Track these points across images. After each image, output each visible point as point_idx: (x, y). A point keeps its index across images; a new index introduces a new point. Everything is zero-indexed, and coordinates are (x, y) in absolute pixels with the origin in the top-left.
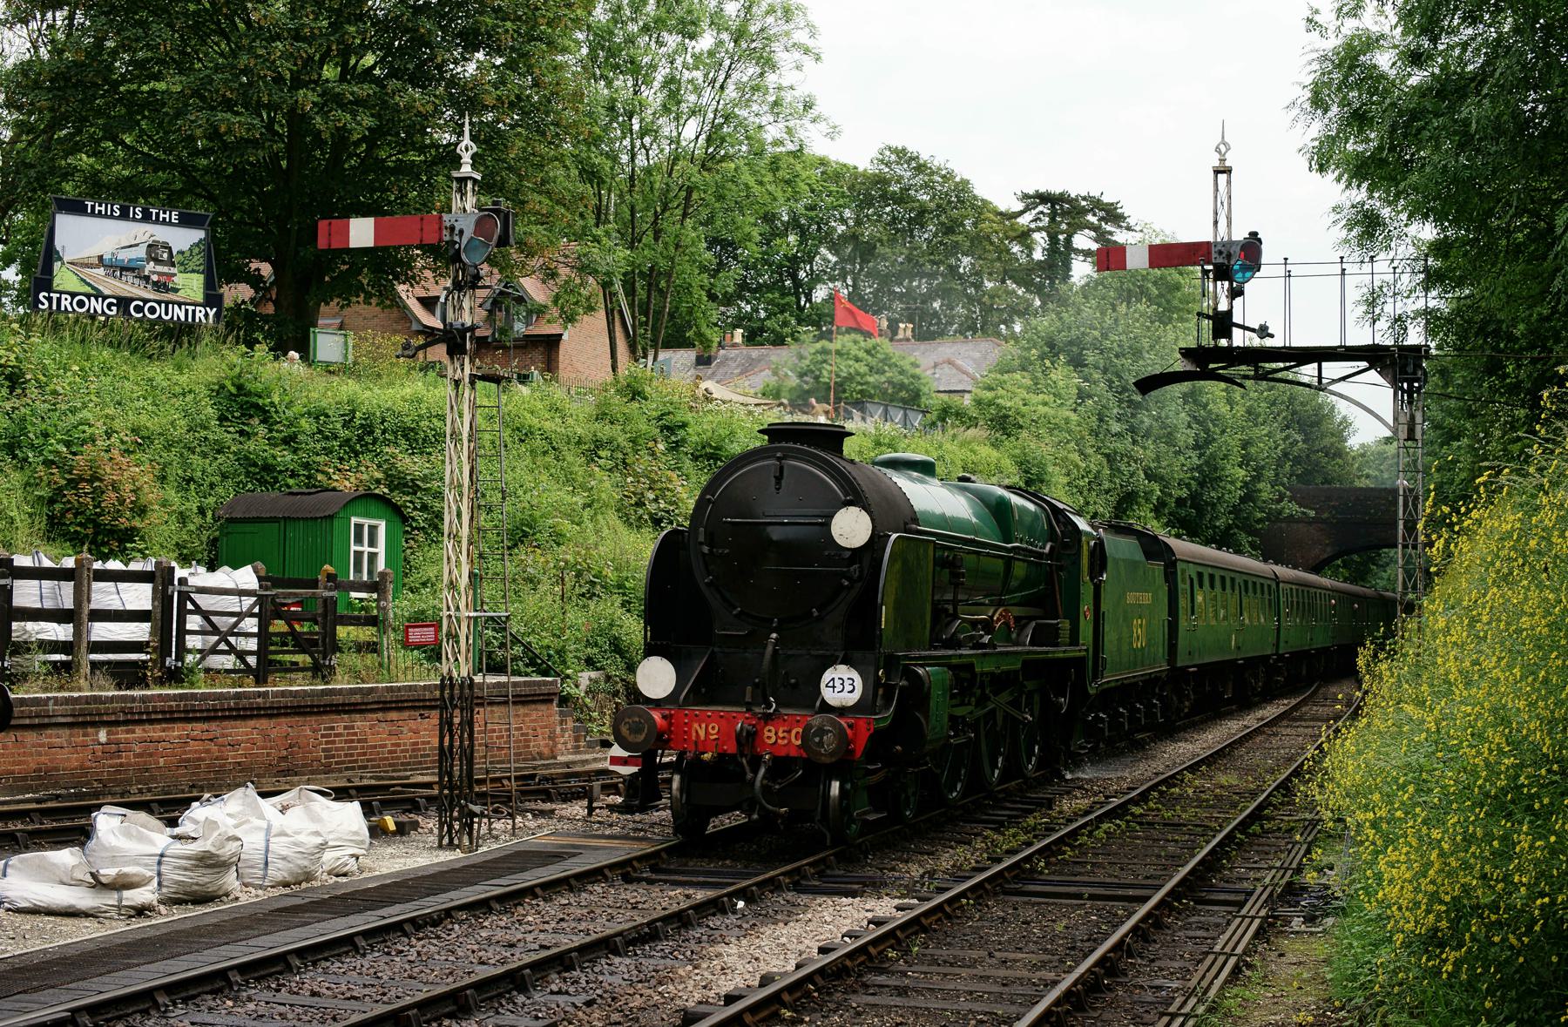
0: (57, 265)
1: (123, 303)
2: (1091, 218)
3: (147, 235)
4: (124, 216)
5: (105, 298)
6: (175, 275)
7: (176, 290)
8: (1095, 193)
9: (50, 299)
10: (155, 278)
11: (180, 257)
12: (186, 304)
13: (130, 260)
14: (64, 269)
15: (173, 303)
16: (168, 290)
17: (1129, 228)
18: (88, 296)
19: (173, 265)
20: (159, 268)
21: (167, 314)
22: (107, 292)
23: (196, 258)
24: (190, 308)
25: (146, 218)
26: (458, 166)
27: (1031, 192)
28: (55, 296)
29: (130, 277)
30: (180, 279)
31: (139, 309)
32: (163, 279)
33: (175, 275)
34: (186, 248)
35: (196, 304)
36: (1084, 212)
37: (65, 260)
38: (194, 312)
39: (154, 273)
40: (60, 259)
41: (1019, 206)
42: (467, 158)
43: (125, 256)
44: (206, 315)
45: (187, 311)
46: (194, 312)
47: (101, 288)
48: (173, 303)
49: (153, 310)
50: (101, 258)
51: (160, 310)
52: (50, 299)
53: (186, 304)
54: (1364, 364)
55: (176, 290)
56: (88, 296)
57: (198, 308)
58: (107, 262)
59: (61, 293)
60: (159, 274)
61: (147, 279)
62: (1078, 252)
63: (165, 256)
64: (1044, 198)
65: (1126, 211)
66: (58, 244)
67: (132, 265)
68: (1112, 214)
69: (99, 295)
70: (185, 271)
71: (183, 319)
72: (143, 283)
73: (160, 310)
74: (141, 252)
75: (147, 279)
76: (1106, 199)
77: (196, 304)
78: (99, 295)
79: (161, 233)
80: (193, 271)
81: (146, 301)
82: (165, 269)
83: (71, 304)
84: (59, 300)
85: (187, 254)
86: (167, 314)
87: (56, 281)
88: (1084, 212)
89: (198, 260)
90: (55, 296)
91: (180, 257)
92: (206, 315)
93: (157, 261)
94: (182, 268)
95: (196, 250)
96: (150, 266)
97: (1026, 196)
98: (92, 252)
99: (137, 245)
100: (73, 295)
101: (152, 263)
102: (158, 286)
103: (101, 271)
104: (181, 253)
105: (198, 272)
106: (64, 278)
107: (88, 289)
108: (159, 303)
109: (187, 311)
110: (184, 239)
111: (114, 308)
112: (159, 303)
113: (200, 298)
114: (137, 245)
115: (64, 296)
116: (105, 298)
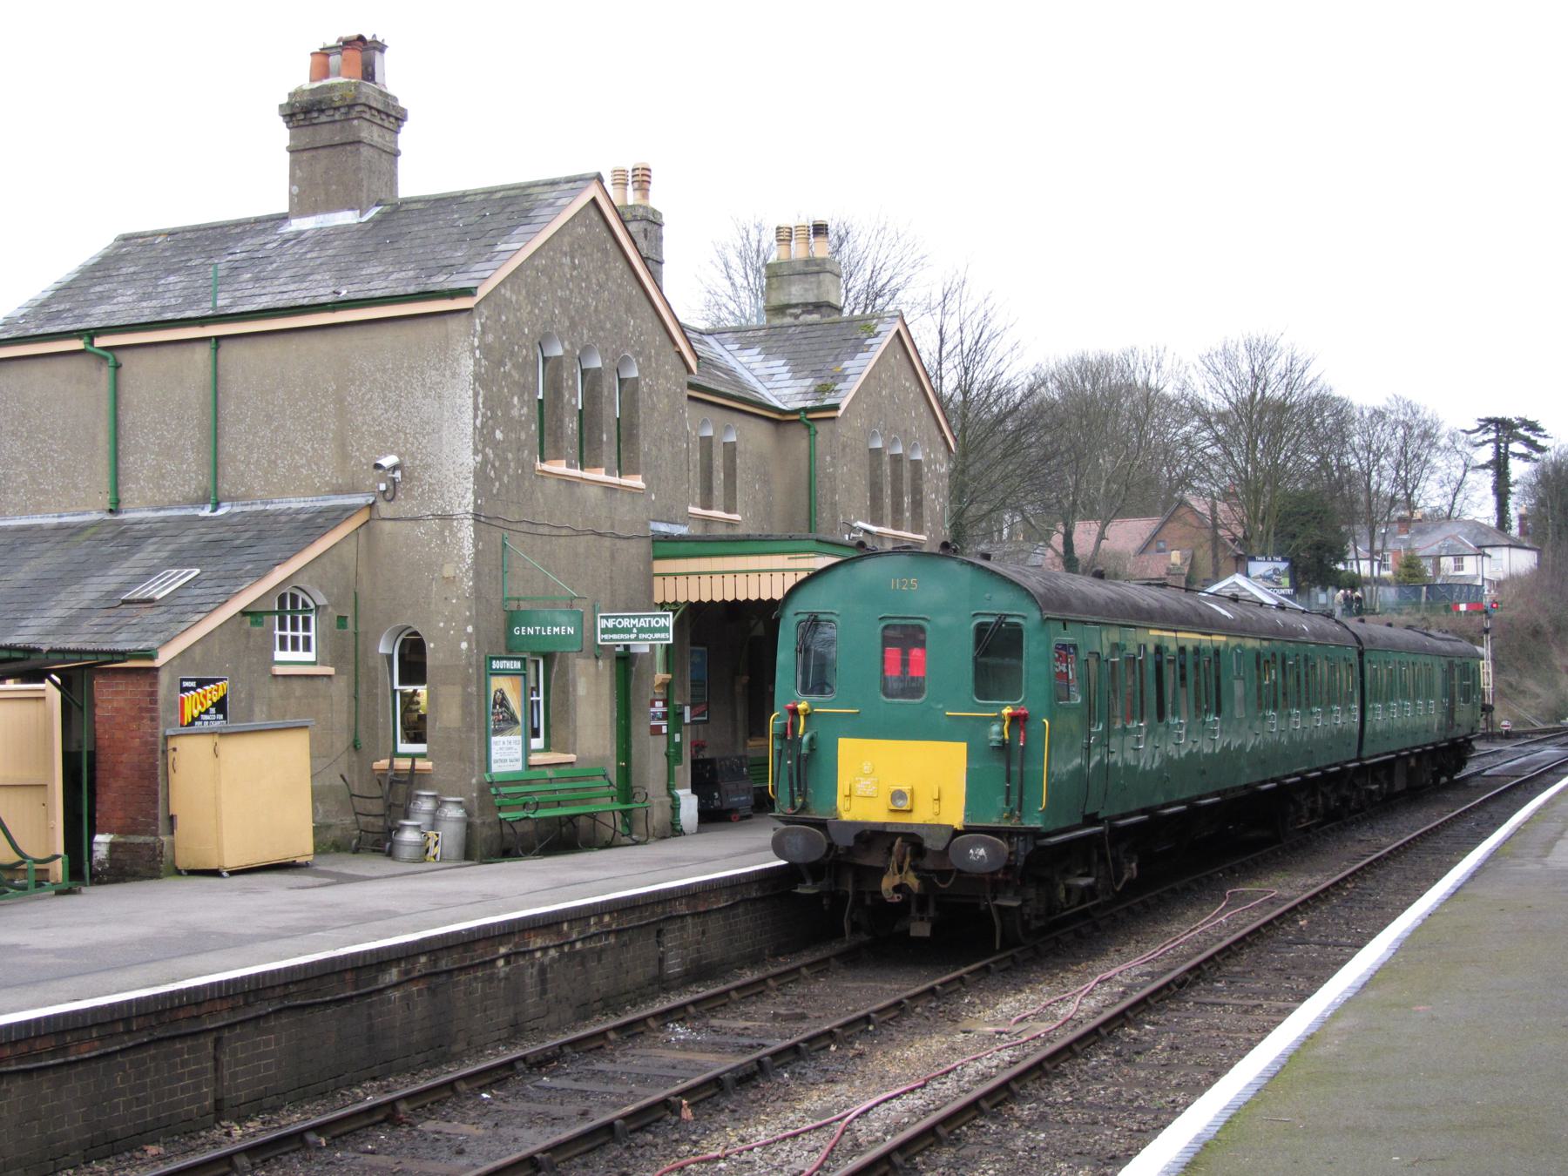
2: (1521, 431)
4: (1266, 560)
8: (1522, 416)
17: (1545, 436)
25: (1272, 560)
27: (1483, 417)
36: (1516, 427)
41: (1477, 427)
43: (1267, 574)
62: (1515, 455)
64: (1490, 421)
65: (1541, 425)
68: (1533, 427)
74: (1271, 572)
76: (1529, 419)
79: (1277, 565)
88: (1516, 427)
89: (1287, 573)
97: (1480, 420)
98: (1258, 574)
102: (1277, 583)
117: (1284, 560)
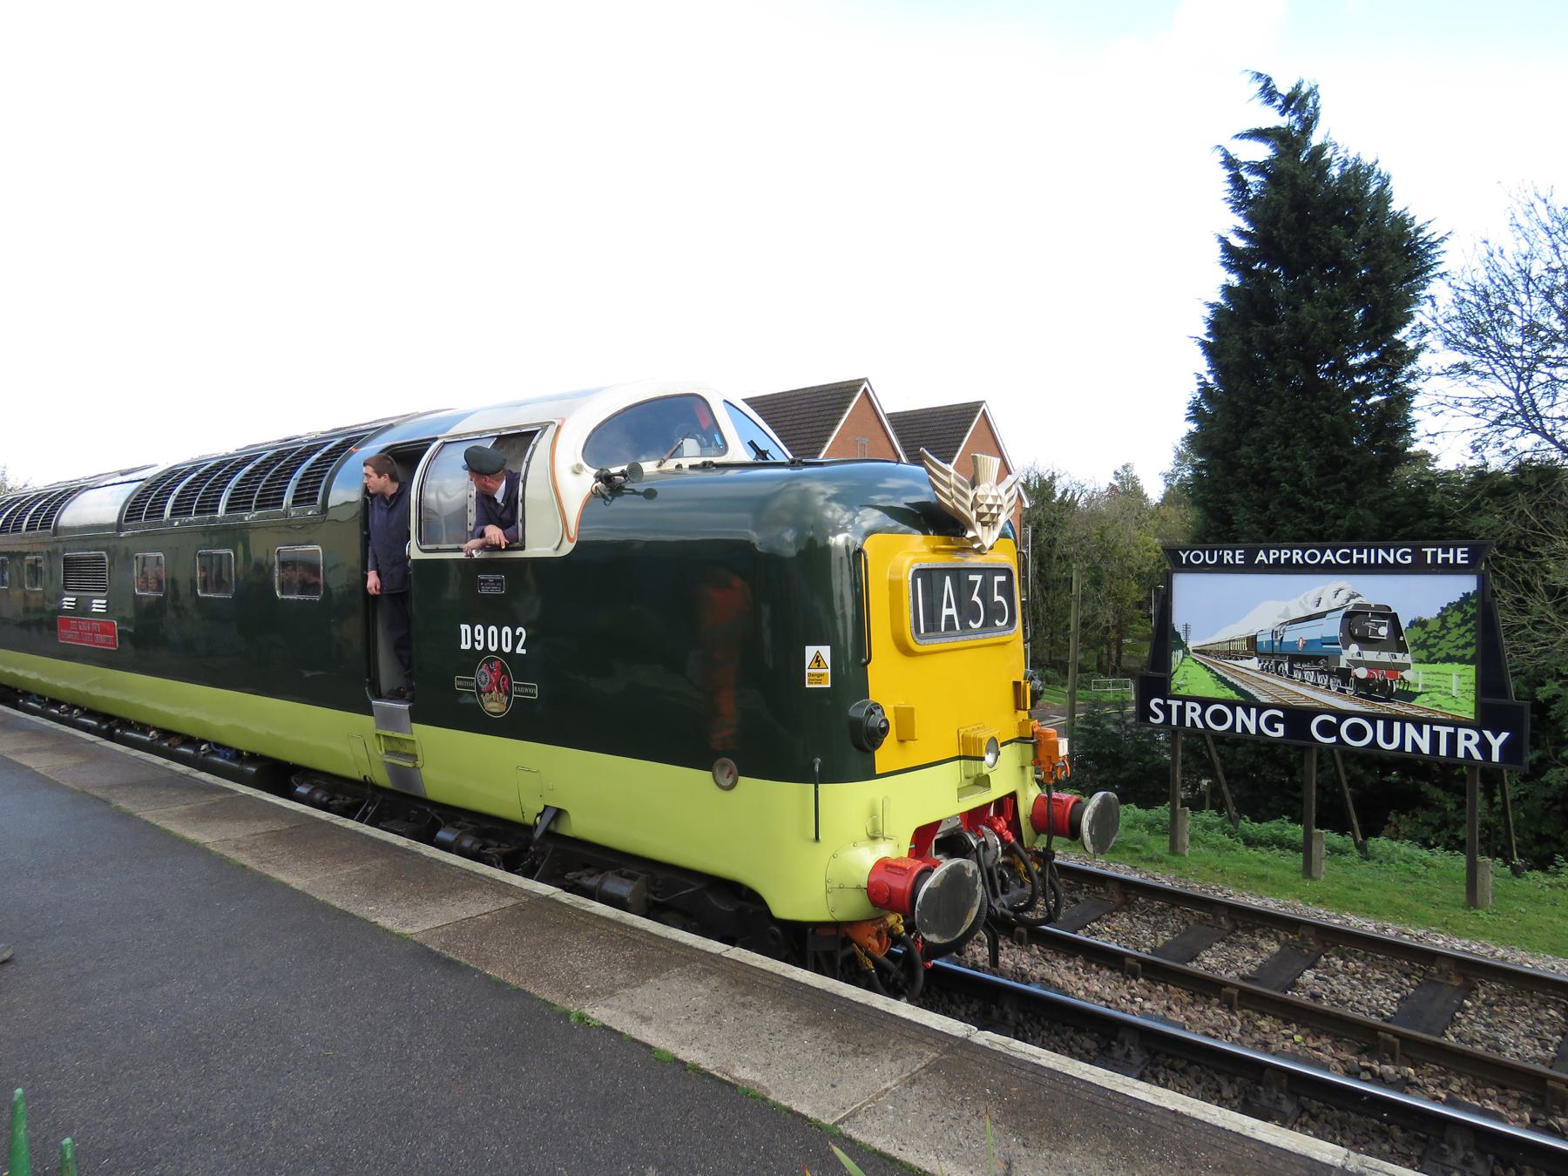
1: (1297, 718)
3: (1343, 596)
5: (1262, 708)
6: (1407, 666)
7: (1410, 696)
10: (1362, 673)
11: (1418, 633)
12: (1432, 722)
13: (1308, 643)
14: (1188, 661)
15: (1404, 720)
16: (1390, 696)
18: (1232, 705)
19: (1402, 648)
20: (1370, 656)
21: (1389, 738)
22: (1264, 699)
23: (1455, 633)
24: (1444, 731)
28: (1175, 704)
30: (1416, 675)
31: (1326, 729)
32: (1379, 675)
33: (1407, 666)
35: (1465, 724)
37: (1191, 645)
38: (1452, 739)
39: (1358, 664)
40: (1182, 645)
43: (1297, 636)
44: (1484, 746)
45: (1435, 737)
46: (1452, 739)
47: (1252, 691)
48: (1404, 720)
49: (1356, 732)
50: (1252, 641)
52: (1166, 709)
53: (1432, 722)
56: (1232, 705)
57: (1462, 732)
58: (1264, 648)
59: (1185, 699)
60: (1370, 665)
61: (1344, 675)
63: (1383, 631)
67: (1314, 651)
69: (1248, 703)
70: (1430, 660)
71: (1425, 748)
72: (1335, 683)
74: (1331, 627)
77: (1457, 723)
78: (1248, 703)
80: (1449, 659)
81: (1342, 715)
82: (1385, 657)
83: (1202, 717)
84: (1181, 710)
85: (1436, 626)
86: (1389, 738)
87: (1177, 680)
90: (1175, 704)
91: (1418, 633)
92: (1484, 746)
93: (1366, 642)
94: (1423, 654)
95: (1457, 617)
98: (1237, 630)
99: (1322, 615)
100: (1205, 703)
101: (1354, 648)
102: (1367, 689)
103: (1253, 663)
104: (1420, 624)
105: (1461, 660)
106: (1190, 677)
107: (1230, 694)
108: (1372, 719)
109: (1435, 737)
111: (1280, 727)
112: (1372, 719)
113: (1467, 710)
114: (1322, 615)
115: (1189, 705)
116: (1262, 708)
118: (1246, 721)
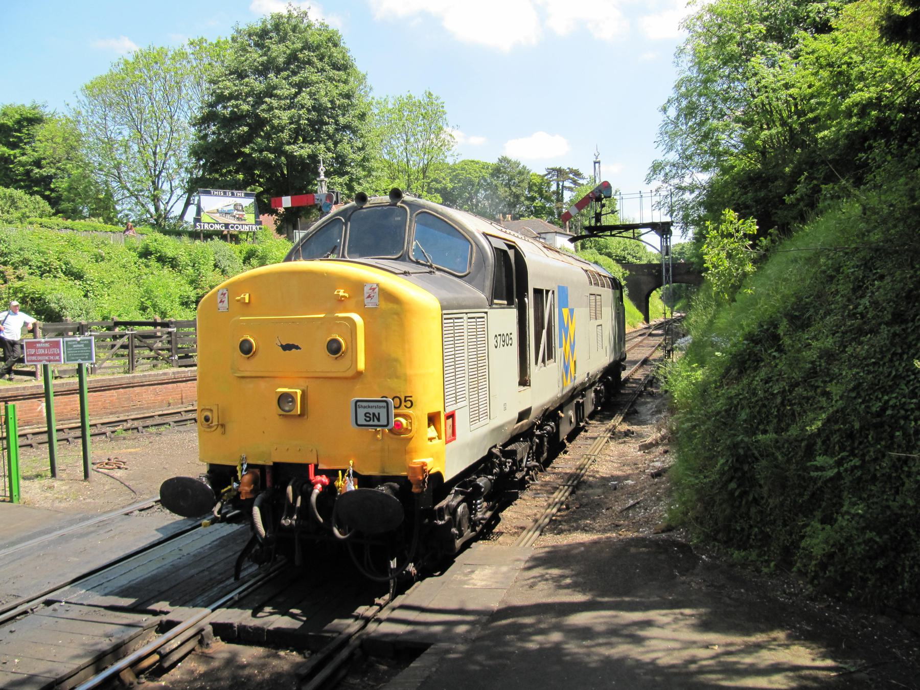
0: (202, 213)
1: (227, 226)
7: (245, 220)
9: (200, 225)
16: (242, 220)
20: (239, 213)
25: (233, 194)
26: (319, 177)
29: (228, 216)
30: (246, 216)
31: (232, 227)
34: (248, 205)
42: (322, 174)
43: (226, 209)
49: (237, 227)
51: (240, 227)
52: (200, 225)
54: (650, 229)
55: (245, 220)
61: (234, 216)
66: (202, 206)
73: (240, 227)
74: (232, 207)
75: (234, 216)
89: (252, 209)
96: (236, 212)
98: (214, 208)
100: (209, 223)
103: (218, 215)
106: (205, 218)
110: (248, 202)
117: (247, 195)
118: (217, 227)
